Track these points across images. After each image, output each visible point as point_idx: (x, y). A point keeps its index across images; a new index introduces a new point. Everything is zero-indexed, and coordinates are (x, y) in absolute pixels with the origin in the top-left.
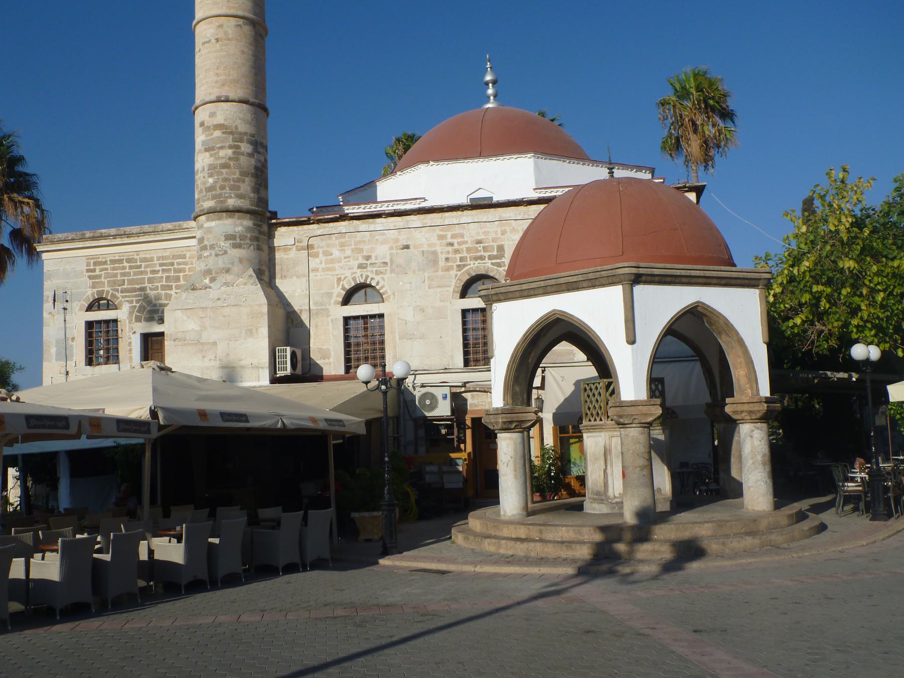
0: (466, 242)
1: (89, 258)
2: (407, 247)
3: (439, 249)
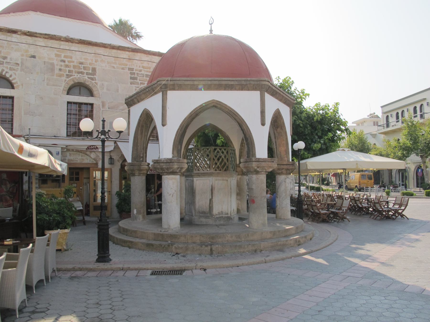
0: (73, 62)
2: (34, 57)
3: (55, 62)
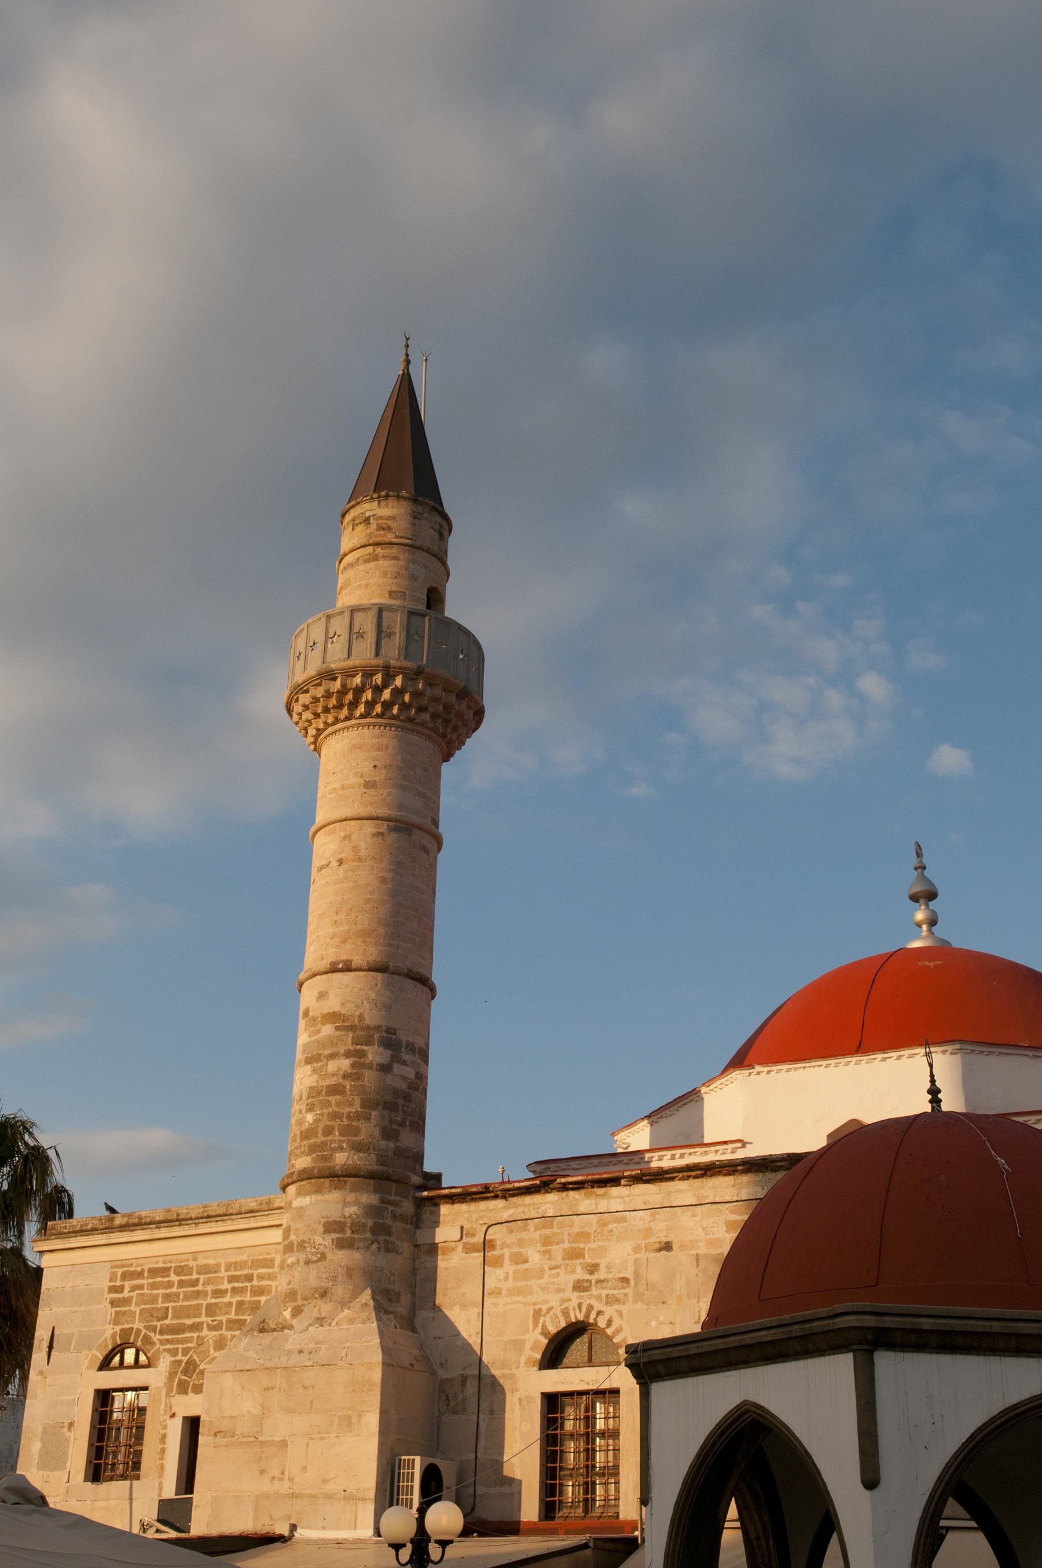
1: (115, 1264)
2: (667, 1247)
